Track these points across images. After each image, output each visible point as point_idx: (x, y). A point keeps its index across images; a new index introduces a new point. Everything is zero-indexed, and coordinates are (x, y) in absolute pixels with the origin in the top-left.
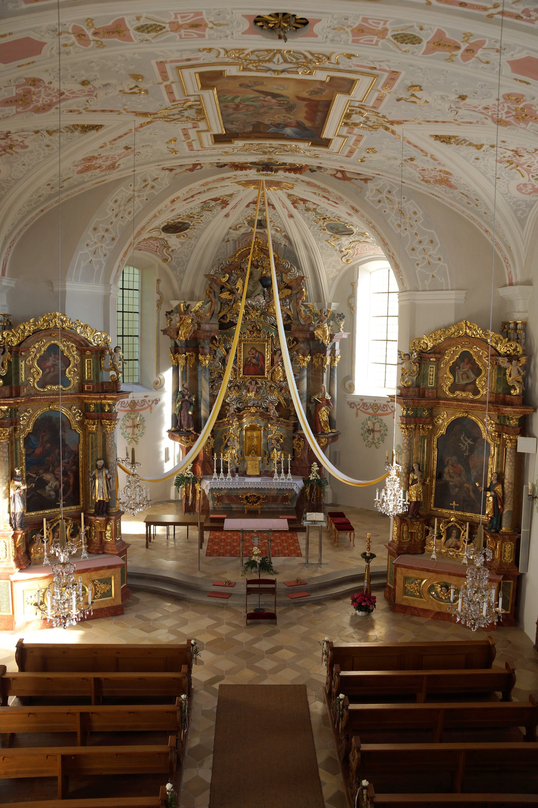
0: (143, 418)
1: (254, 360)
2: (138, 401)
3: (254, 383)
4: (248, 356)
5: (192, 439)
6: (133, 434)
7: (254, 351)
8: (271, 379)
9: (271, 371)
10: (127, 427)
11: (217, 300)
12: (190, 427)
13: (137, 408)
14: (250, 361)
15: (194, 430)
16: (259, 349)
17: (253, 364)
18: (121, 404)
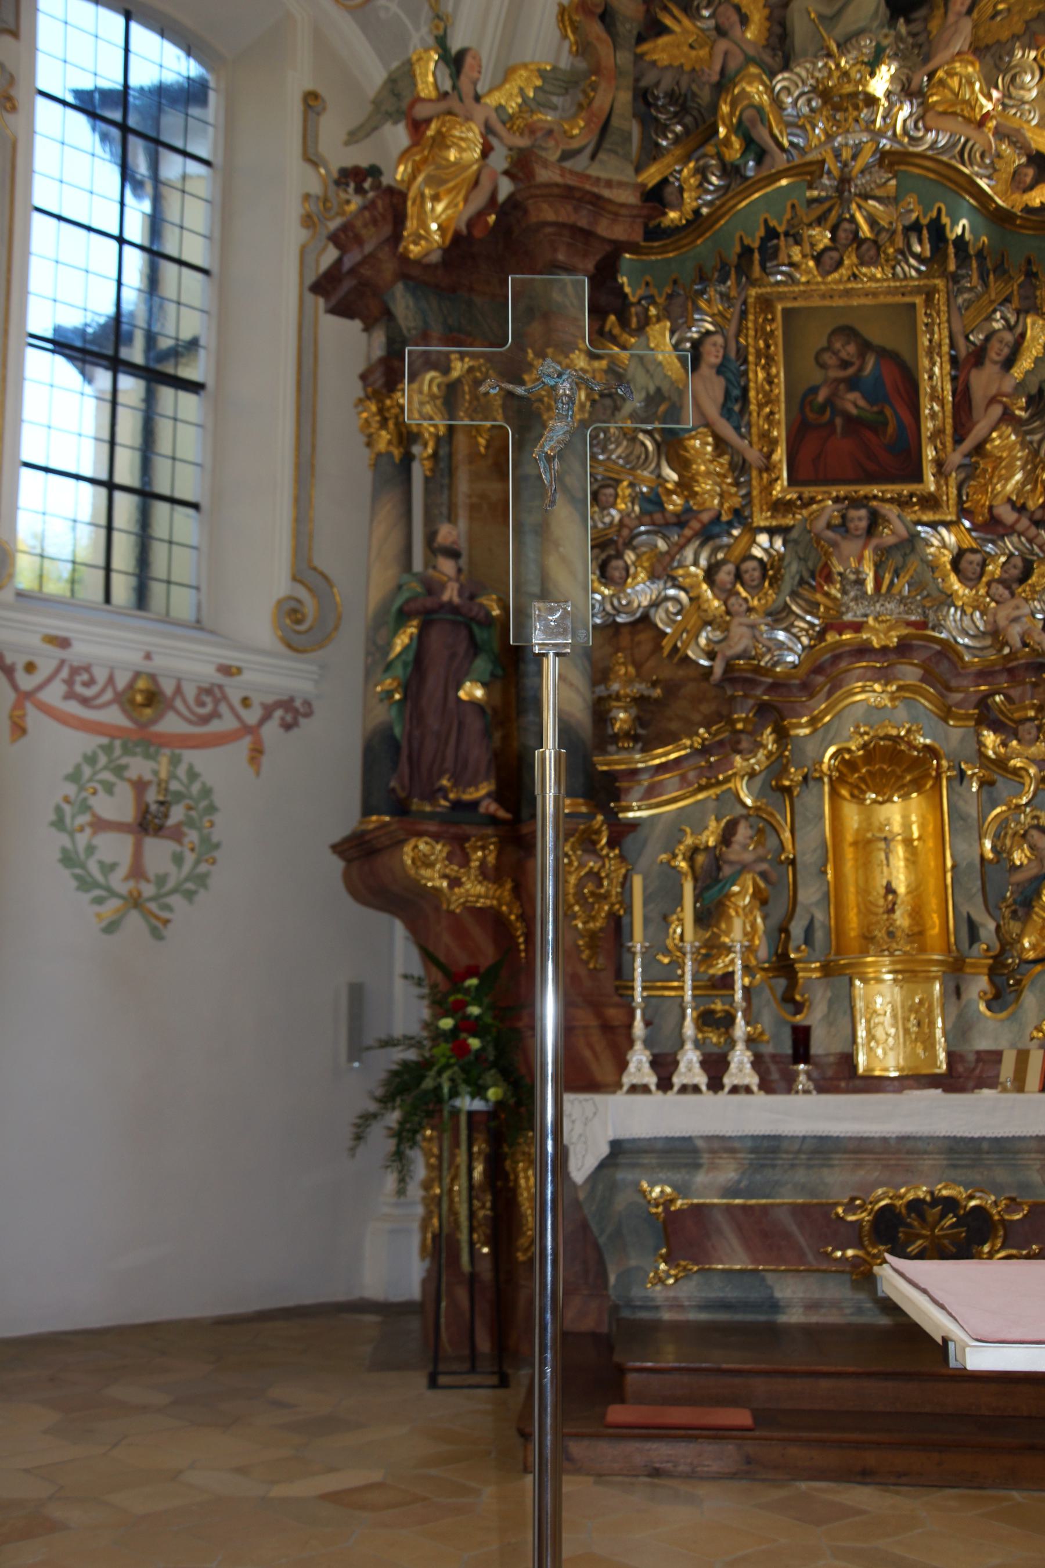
0: (206, 792)
1: (853, 396)
2: (178, 690)
3: (859, 517)
4: (816, 376)
5: (483, 861)
6: (137, 872)
7: (851, 349)
8: (963, 512)
9: (956, 458)
10: (100, 825)
11: (624, 58)
12: (474, 783)
13: (171, 724)
14: (829, 402)
15: (498, 796)
16: (877, 334)
17: (848, 418)
18: (70, 682)
